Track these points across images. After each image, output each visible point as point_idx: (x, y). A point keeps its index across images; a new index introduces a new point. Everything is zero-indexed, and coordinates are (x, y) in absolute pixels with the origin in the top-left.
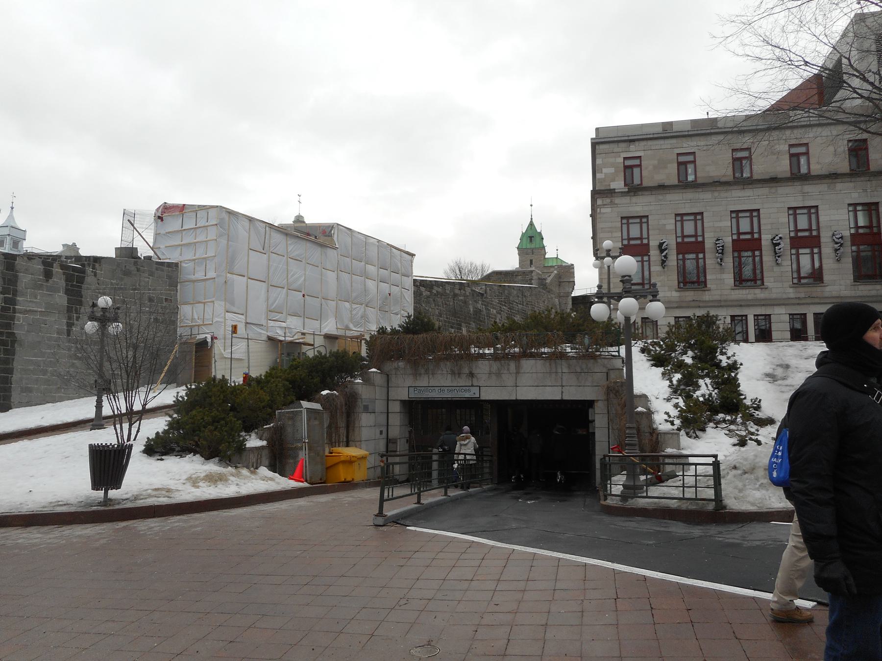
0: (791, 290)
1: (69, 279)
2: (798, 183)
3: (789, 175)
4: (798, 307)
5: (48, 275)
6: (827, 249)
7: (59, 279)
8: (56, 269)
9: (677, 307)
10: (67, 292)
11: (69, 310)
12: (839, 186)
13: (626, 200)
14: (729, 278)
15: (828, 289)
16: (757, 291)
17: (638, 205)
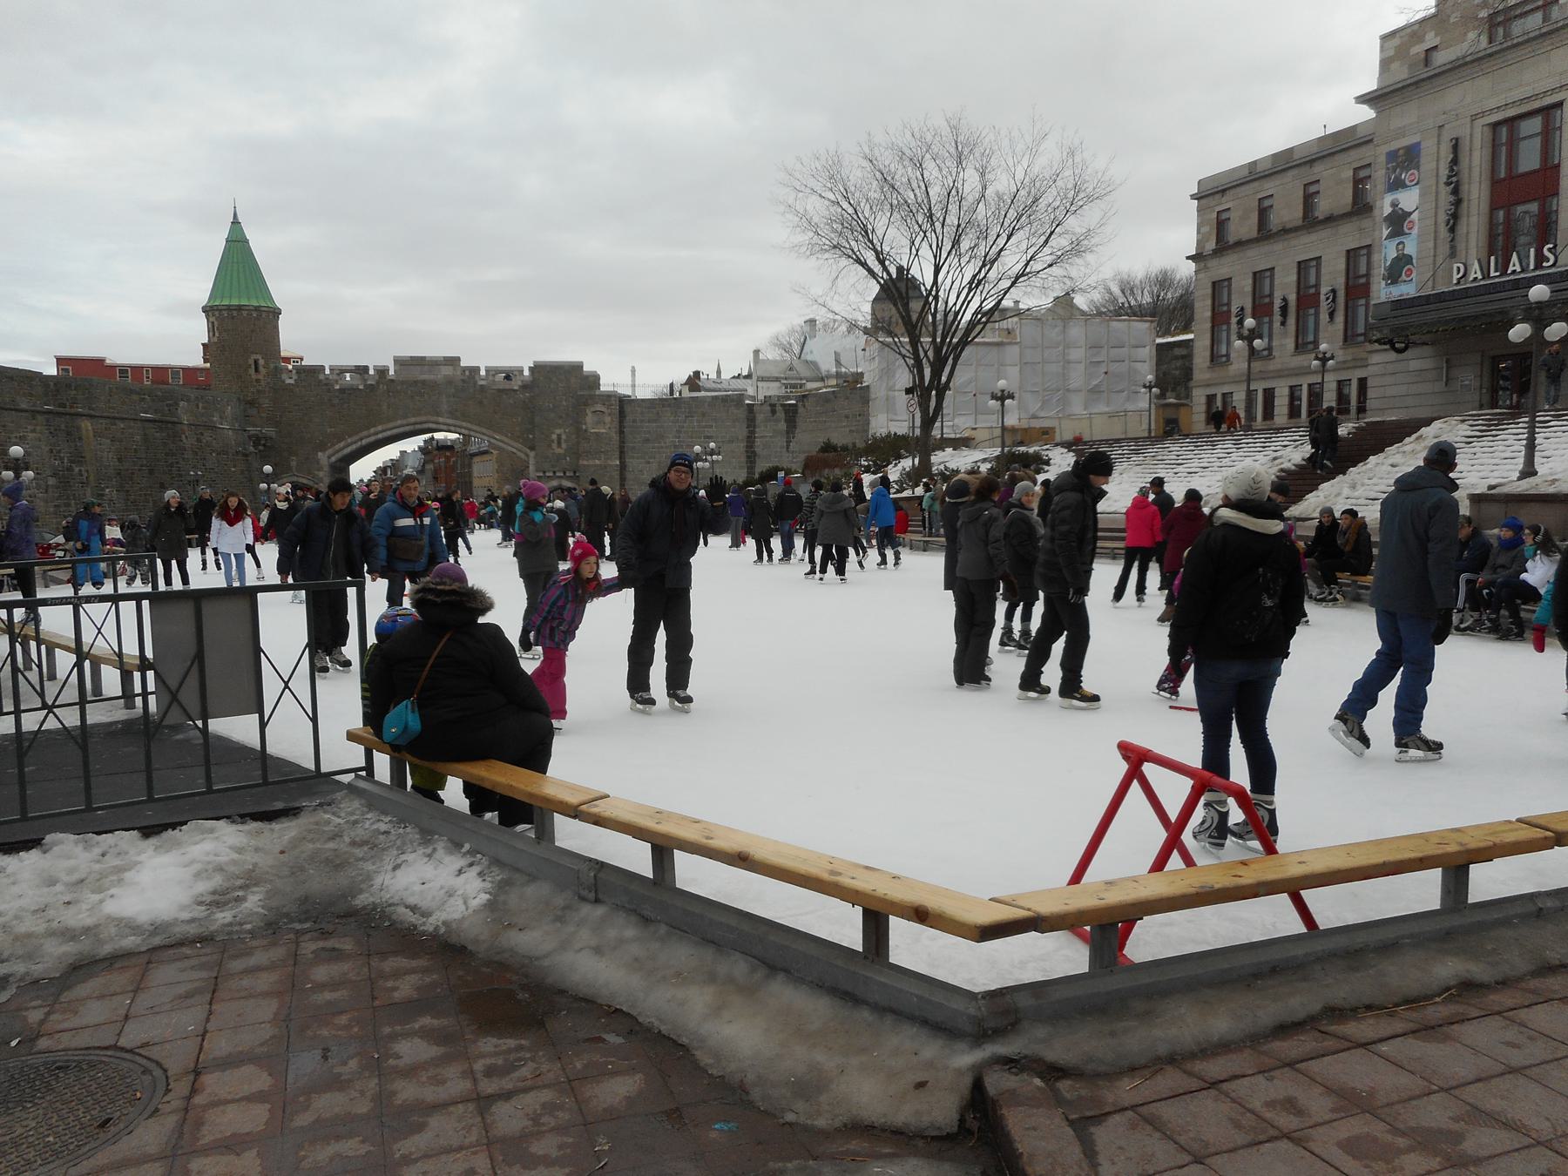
1: (786, 412)
2: (1355, 218)
5: (774, 412)
7: (781, 414)
8: (779, 408)
10: (786, 421)
11: (788, 432)
14: (1290, 343)
17: (1221, 268)
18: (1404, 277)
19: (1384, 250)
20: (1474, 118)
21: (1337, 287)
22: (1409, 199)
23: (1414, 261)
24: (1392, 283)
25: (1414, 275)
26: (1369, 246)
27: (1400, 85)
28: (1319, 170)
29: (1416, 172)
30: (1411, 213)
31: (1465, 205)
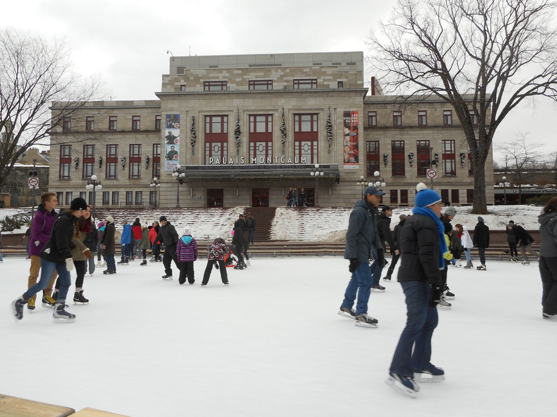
0: (128, 181)
3: (131, 130)
4: (130, 189)
6: (143, 163)
9: (81, 188)
12: (150, 136)
13: (63, 137)
14: (103, 175)
15: (142, 181)
16: (114, 181)
18: (174, 158)
19: (166, 147)
20: (199, 112)
21: (126, 157)
22: (176, 132)
23: (178, 154)
24: (169, 160)
25: (178, 158)
26: (139, 145)
27: (165, 94)
28: (116, 112)
29: (178, 124)
30: (176, 137)
31: (197, 138)
